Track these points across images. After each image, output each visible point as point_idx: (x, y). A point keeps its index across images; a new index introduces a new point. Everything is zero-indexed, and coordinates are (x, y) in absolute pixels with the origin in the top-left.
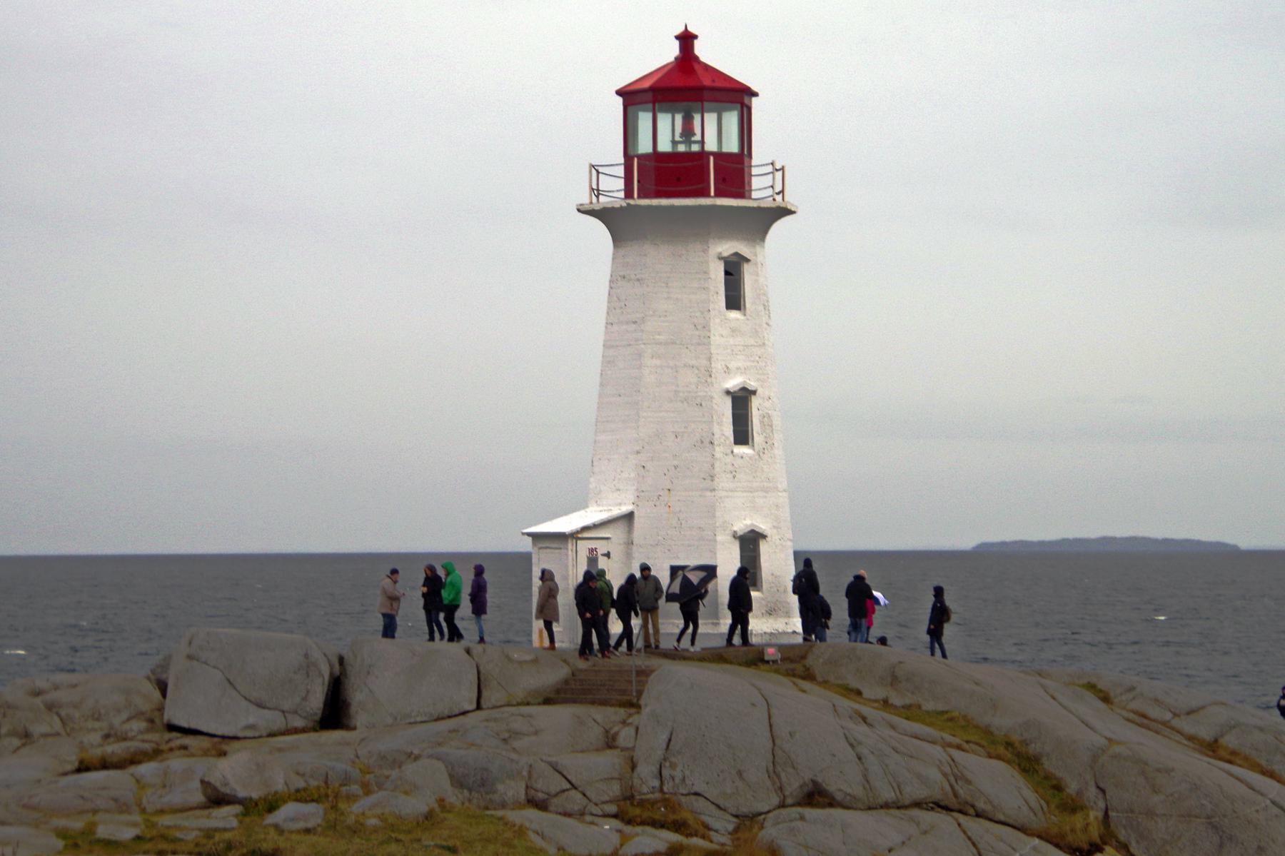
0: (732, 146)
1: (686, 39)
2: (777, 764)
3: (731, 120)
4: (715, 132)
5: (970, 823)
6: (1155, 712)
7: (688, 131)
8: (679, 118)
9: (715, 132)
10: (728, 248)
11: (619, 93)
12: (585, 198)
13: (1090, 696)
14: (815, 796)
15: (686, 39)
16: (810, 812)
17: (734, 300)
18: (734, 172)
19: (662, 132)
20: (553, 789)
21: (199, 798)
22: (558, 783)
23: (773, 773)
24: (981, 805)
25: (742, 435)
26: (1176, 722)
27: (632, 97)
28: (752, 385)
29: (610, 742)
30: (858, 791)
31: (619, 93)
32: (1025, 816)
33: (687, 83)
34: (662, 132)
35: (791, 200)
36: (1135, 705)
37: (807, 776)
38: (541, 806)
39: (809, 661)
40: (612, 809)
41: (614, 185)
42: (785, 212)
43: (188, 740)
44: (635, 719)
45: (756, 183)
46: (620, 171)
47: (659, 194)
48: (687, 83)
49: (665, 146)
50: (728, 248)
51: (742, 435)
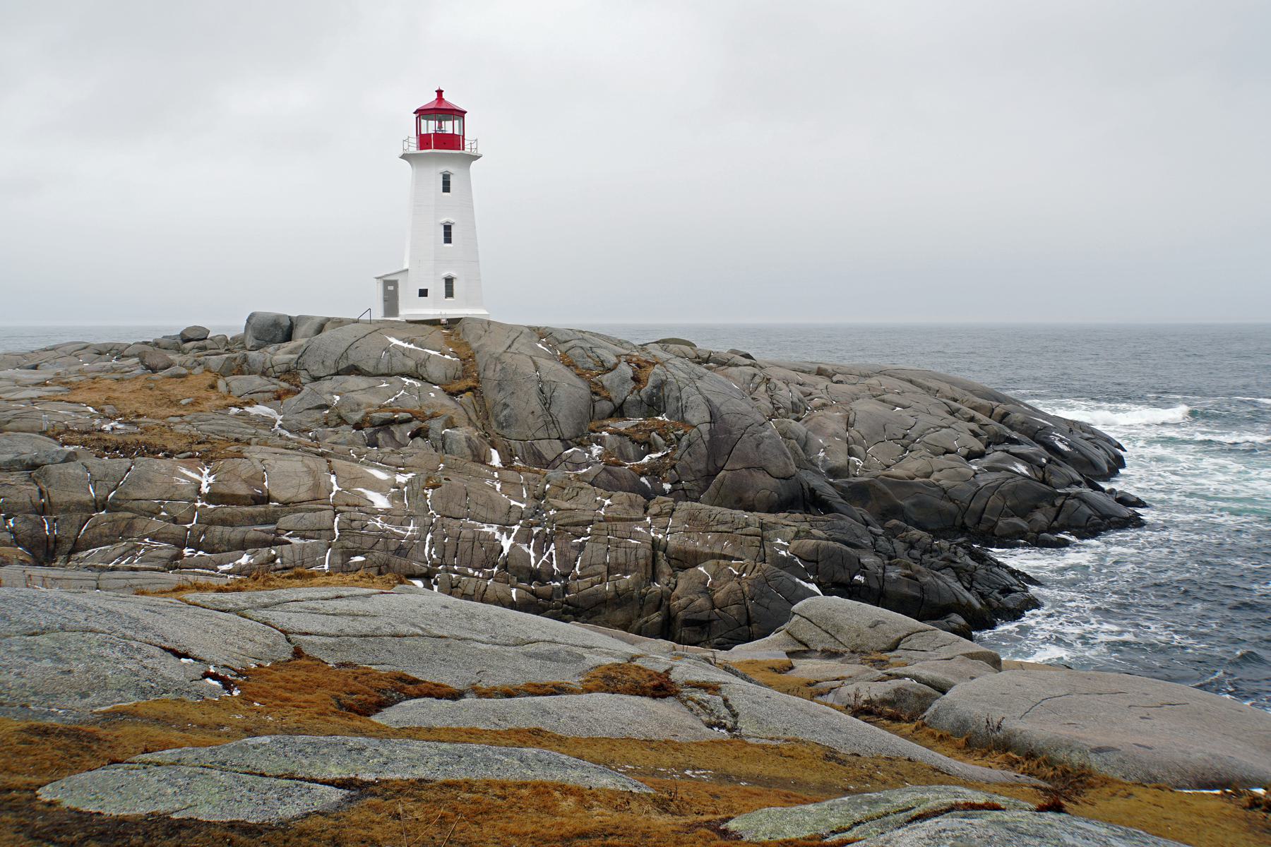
1: (440, 92)
4: (449, 127)
7: (440, 127)
10: (444, 168)
12: (401, 153)
14: (354, 370)
15: (440, 92)
17: (446, 188)
18: (452, 142)
19: (430, 127)
23: (337, 362)
25: (448, 239)
28: (452, 220)
30: (371, 370)
33: (440, 110)
34: (430, 127)
35: (480, 152)
37: (351, 362)
41: (413, 148)
42: (477, 157)
46: (414, 140)
48: (440, 110)
50: (444, 168)
51: (448, 239)
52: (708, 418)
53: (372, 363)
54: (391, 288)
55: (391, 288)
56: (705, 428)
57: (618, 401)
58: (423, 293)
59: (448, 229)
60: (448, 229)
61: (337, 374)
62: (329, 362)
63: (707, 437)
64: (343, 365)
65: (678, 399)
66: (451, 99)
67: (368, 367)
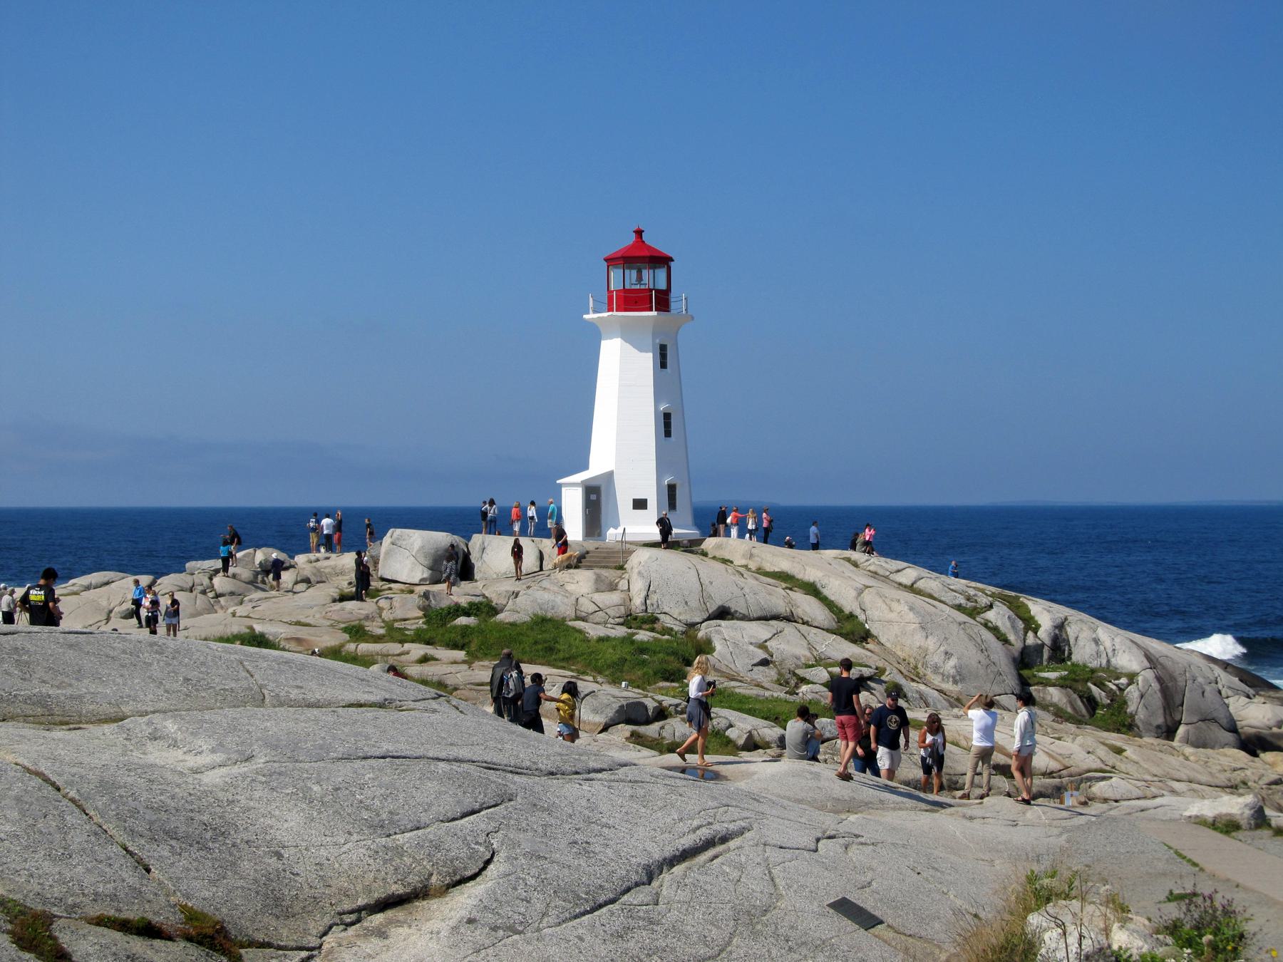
0: (662, 285)
1: (639, 233)
2: (704, 596)
3: (661, 274)
4: (654, 279)
5: (804, 628)
6: (881, 572)
7: (640, 278)
8: (634, 273)
9: (654, 279)
11: (606, 260)
13: (847, 564)
14: (723, 613)
15: (639, 233)
16: (723, 623)
20: (590, 611)
21: (1224, 722)
22: (592, 608)
24: (806, 619)
26: (892, 577)
27: (611, 261)
29: (613, 587)
30: (744, 611)
31: (606, 260)
32: (826, 624)
36: (872, 568)
37: (720, 603)
38: (584, 619)
39: (703, 546)
40: (621, 620)
43: (392, 585)
44: (626, 576)
45: (673, 306)
47: (626, 310)
49: (627, 287)
52: (1148, 665)
53: (742, 601)
54: (593, 497)
55: (593, 497)
56: (1150, 674)
57: (1018, 645)
58: (640, 504)
59: (667, 417)
60: (667, 417)
61: (709, 619)
62: (694, 603)
63: (1156, 686)
64: (712, 608)
65: (1097, 641)
67: (737, 606)
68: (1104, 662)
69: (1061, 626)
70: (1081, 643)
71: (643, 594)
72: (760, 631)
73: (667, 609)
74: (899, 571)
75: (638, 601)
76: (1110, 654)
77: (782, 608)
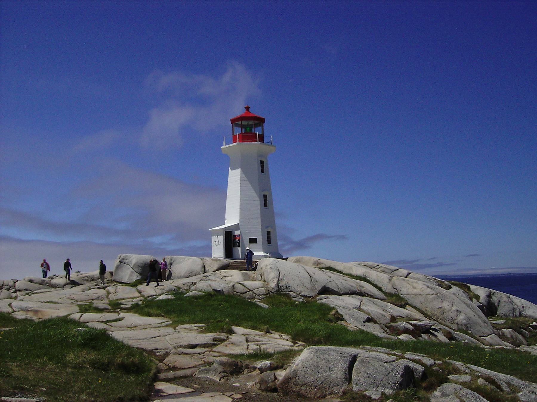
1: (247, 108)
37: (323, 285)
62: (308, 285)
64: (319, 288)
65: (512, 303)
66: (256, 112)
67: (332, 286)
68: (518, 314)
69: (489, 296)
70: (502, 304)
71: (276, 280)
72: (353, 301)
73: (293, 289)
74: (395, 270)
75: (272, 285)
76: (522, 309)
77: (356, 288)
